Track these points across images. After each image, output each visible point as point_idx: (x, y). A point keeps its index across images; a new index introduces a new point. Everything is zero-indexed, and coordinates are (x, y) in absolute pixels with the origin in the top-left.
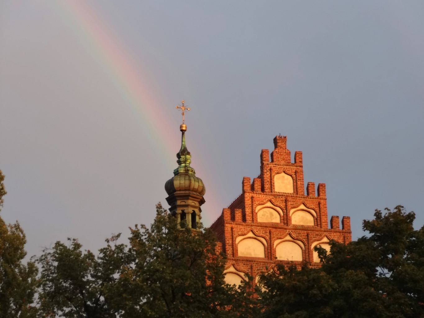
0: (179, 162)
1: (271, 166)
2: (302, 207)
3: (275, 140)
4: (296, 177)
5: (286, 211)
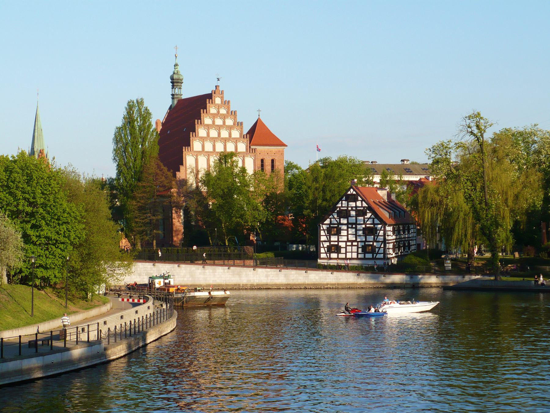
0: (175, 69)
1: (215, 95)
2: (223, 108)
3: (216, 86)
4: (222, 98)
5: (219, 109)
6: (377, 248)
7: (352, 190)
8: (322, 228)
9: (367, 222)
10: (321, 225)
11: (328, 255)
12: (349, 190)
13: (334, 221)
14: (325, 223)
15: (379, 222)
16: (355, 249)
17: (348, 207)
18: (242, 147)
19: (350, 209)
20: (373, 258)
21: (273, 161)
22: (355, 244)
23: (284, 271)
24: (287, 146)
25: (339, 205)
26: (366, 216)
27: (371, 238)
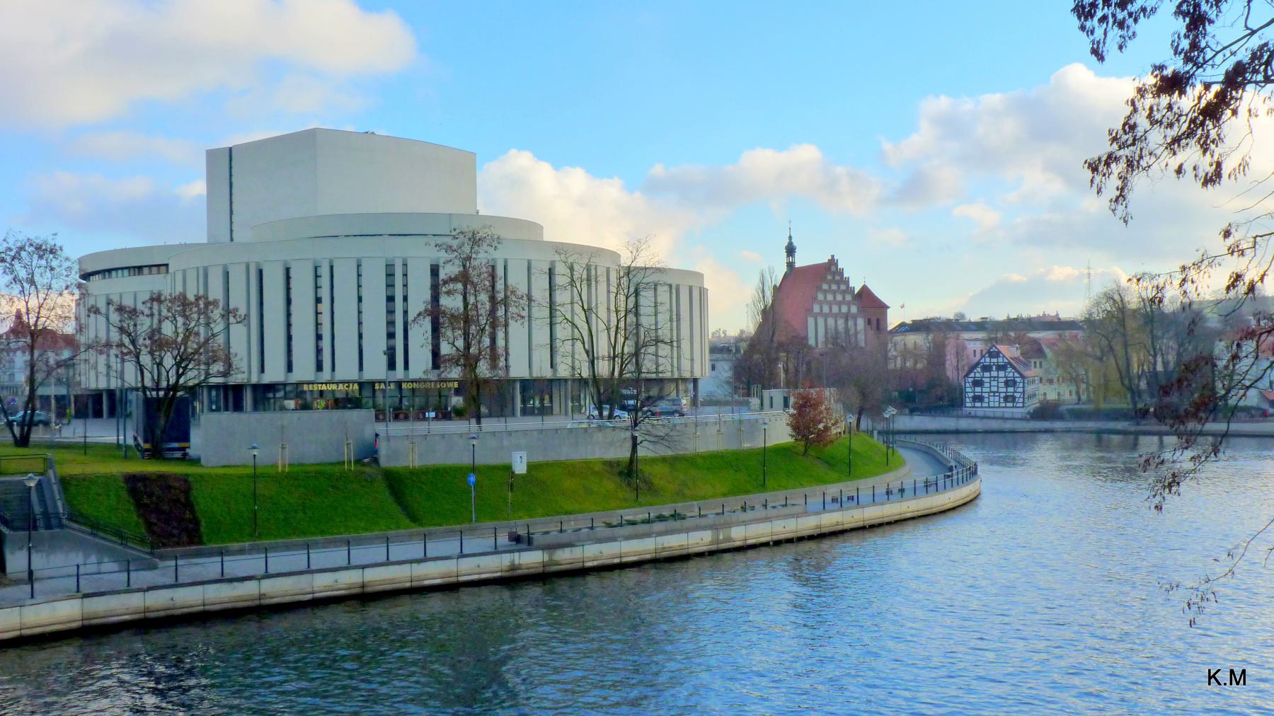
13: (978, 375)
16: (997, 399)
18: (854, 309)
20: (1013, 407)
21: (878, 320)
22: (997, 394)
23: (938, 419)
24: (889, 307)
25: (983, 361)
27: (1010, 389)
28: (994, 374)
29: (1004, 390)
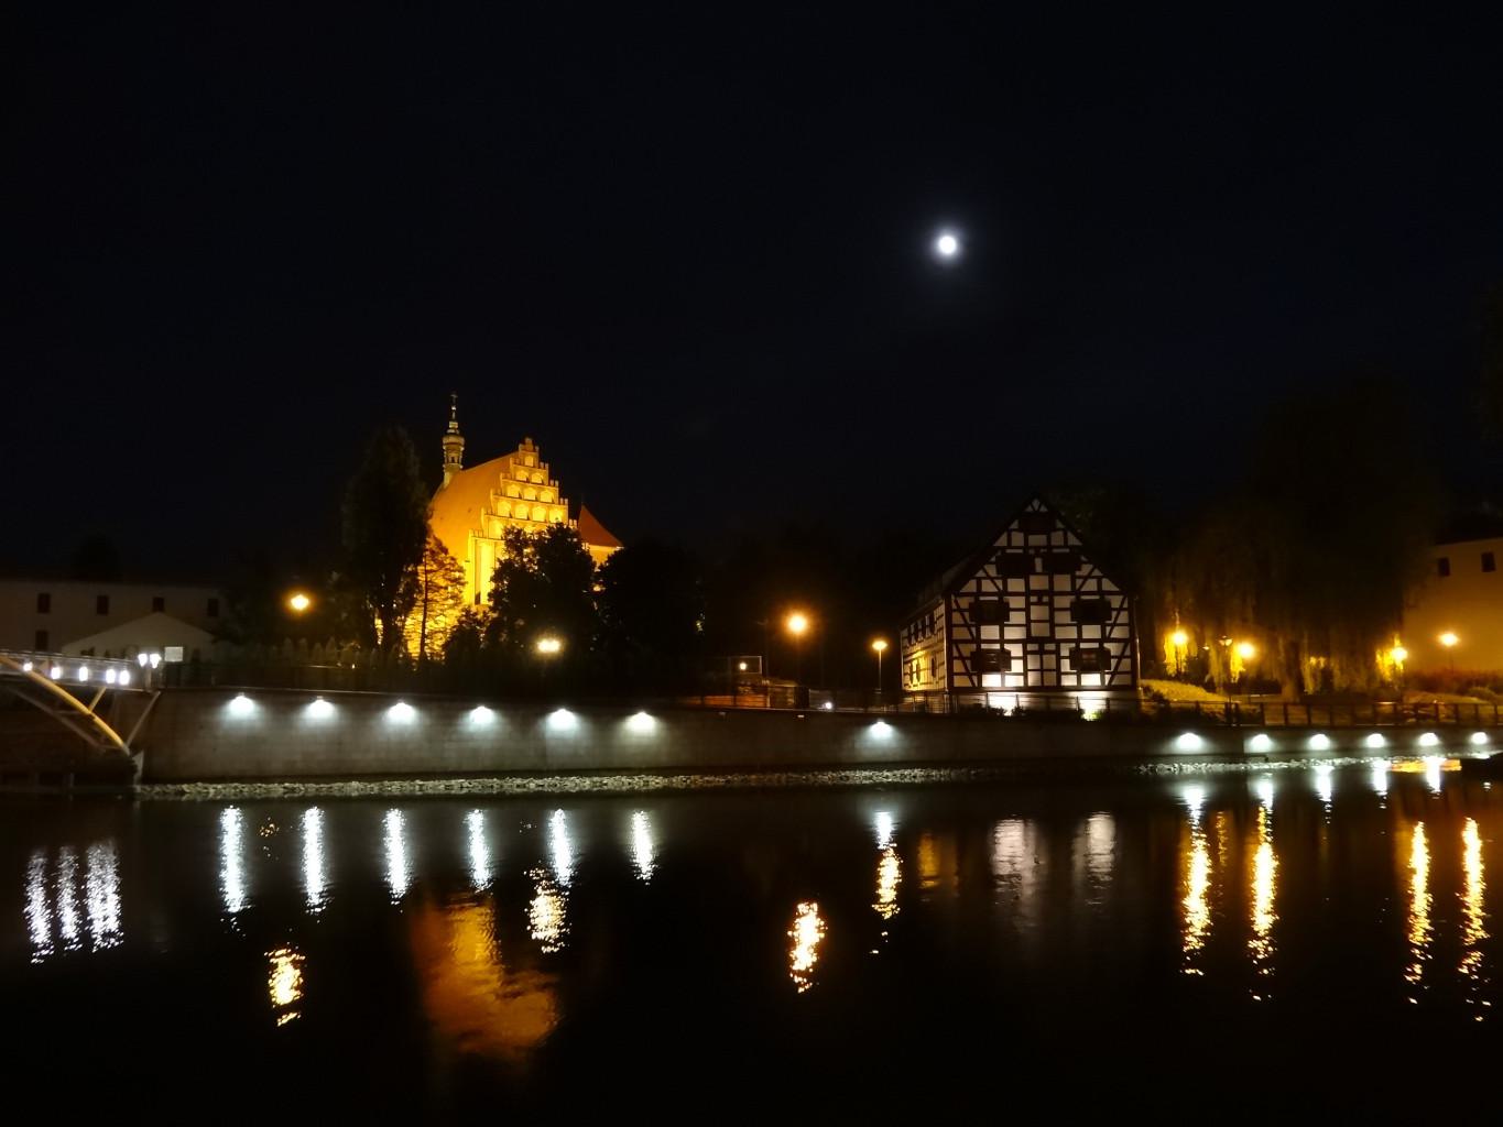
6: (1113, 657)
7: (1036, 503)
8: (954, 606)
9: (1081, 586)
10: (953, 597)
11: (975, 679)
12: (1031, 503)
13: (987, 586)
14: (964, 590)
15: (1116, 589)
17: (1026, 547)
19: (1032, 552)
22: (1052, 647)
25: (1002, 541)
26: (1080, 570)
27: (1092, 631)
28: (1038, 583)
29: (1072, 633)
